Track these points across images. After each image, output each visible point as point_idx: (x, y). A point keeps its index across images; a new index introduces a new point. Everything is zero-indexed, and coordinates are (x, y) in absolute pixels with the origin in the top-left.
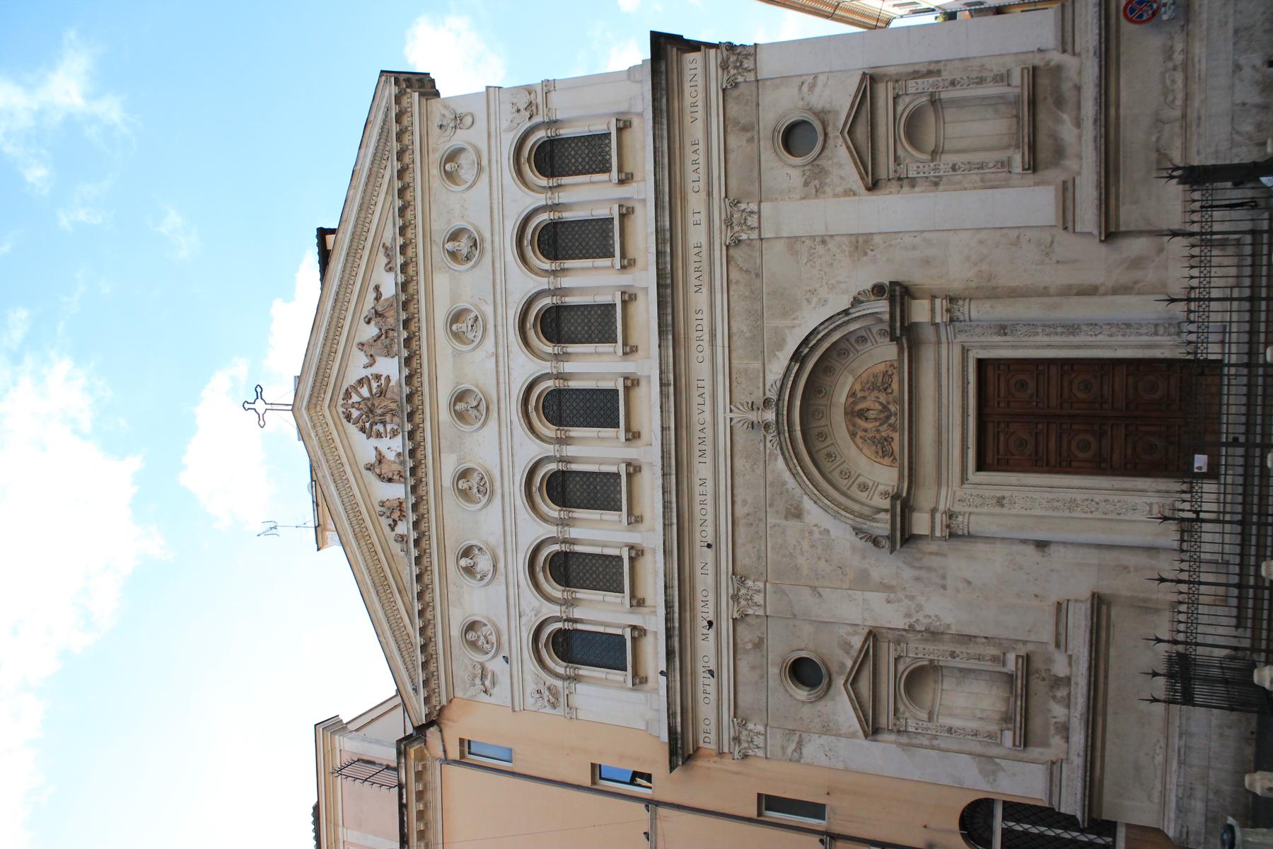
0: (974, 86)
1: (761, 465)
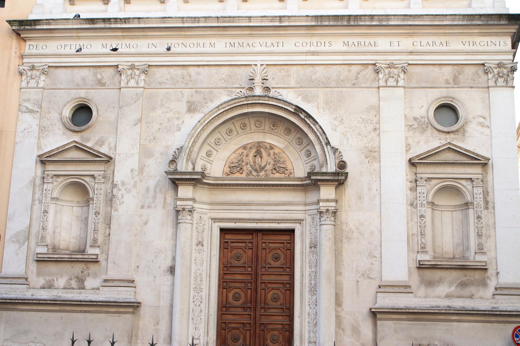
0: (476, 231)
1: (225, 85)
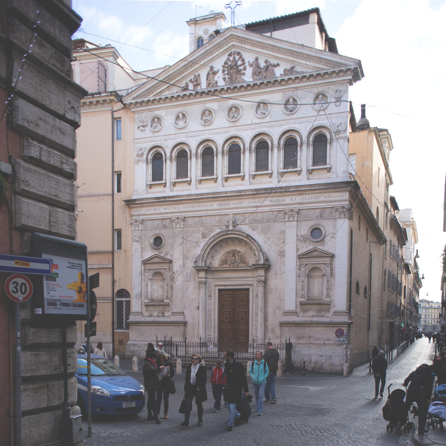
1: (217, 224)
